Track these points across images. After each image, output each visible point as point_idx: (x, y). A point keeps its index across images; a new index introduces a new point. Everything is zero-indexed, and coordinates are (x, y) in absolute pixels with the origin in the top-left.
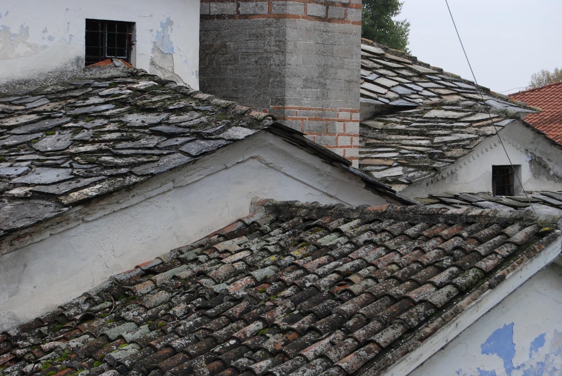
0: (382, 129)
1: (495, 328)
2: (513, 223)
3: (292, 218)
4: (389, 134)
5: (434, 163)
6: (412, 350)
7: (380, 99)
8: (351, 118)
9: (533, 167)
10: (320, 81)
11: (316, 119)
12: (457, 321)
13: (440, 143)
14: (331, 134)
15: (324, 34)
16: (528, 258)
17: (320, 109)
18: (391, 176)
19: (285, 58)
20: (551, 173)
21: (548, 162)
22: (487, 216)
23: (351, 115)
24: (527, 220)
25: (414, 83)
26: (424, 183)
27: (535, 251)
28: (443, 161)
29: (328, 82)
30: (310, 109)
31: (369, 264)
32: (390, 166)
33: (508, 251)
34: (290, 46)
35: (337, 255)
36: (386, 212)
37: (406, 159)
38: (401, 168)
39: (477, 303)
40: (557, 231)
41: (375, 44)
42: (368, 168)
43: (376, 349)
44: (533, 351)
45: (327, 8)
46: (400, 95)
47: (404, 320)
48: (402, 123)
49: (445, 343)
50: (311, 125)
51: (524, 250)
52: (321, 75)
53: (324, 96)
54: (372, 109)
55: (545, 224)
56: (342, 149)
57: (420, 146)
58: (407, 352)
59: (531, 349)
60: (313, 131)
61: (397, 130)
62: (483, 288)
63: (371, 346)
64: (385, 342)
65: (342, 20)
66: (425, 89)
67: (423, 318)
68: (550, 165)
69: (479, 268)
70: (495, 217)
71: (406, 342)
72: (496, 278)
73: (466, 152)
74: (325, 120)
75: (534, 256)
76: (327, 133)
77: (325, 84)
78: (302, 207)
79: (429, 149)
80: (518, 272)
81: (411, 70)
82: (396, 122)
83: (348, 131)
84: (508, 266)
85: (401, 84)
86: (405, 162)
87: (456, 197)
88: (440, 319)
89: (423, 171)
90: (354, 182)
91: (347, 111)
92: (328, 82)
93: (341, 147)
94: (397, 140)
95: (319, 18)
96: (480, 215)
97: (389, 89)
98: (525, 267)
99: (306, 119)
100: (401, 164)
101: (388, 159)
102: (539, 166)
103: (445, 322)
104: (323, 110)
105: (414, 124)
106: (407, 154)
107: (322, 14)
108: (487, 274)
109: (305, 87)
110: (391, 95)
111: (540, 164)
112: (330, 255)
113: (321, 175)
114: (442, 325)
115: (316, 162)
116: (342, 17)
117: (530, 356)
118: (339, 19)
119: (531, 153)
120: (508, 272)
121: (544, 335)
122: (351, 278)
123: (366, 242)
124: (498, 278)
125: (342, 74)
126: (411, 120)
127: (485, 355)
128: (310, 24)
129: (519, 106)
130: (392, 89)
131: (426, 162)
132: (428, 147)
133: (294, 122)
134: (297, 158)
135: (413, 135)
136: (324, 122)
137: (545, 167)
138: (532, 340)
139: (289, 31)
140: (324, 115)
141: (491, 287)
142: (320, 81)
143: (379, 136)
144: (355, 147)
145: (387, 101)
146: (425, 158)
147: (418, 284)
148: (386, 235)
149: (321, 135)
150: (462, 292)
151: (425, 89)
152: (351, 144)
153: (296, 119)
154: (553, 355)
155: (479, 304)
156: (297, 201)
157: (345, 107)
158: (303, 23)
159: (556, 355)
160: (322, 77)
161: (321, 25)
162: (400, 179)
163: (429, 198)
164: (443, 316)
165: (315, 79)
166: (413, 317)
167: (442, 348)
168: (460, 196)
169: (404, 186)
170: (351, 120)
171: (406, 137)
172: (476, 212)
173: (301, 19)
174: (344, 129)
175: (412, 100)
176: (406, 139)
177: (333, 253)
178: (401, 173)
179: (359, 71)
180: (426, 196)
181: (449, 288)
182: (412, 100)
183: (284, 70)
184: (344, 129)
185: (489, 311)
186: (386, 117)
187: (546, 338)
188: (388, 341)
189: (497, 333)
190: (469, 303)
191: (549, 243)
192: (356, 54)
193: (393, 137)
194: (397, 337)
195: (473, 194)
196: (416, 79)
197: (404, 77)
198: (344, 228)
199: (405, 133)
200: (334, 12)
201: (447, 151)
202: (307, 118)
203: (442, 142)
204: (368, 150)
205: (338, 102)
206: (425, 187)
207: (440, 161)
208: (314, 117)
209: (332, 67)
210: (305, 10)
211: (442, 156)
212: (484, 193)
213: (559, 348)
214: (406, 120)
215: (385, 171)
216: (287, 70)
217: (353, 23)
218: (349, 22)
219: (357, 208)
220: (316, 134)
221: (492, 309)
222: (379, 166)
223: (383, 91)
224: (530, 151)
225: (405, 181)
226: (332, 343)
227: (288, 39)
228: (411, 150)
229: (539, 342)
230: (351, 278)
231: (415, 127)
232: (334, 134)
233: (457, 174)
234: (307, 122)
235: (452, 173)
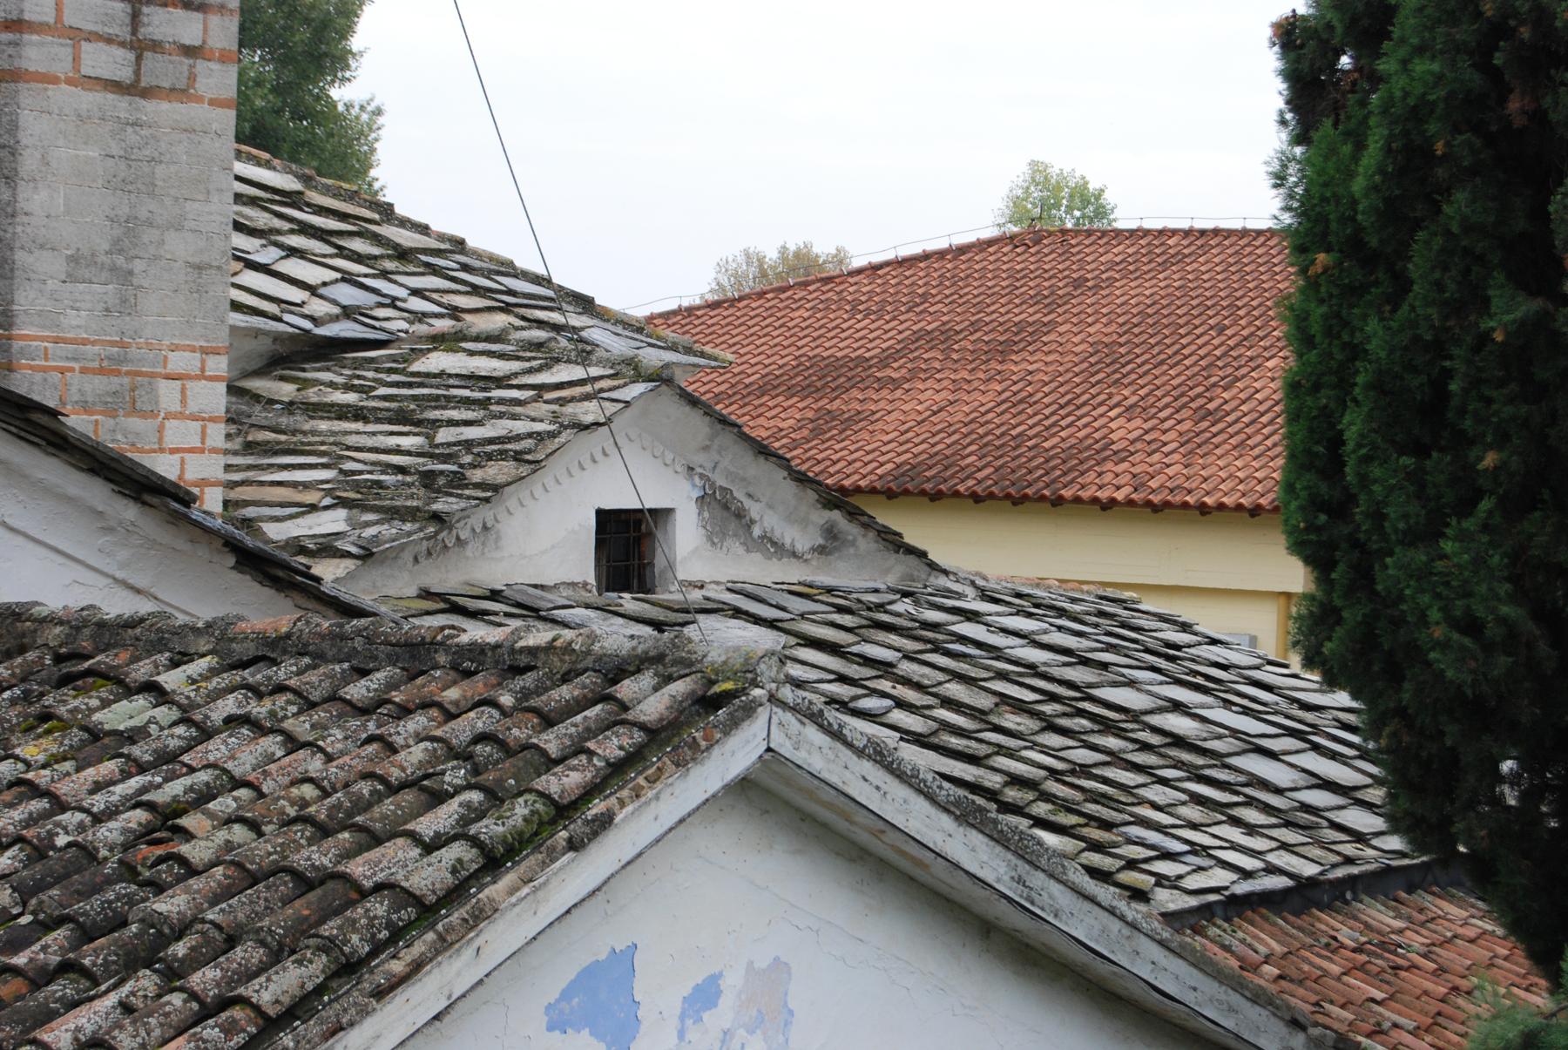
0: (291, 403)
1: (586, 960)
2: (639, 671)
3: (22, 650)
4: (312, 418)
5: (435, 500)
6: (352, 1024)
7: (287, 317)
8: (203, 370)
9: (706, 515)
10: (117, 264)
11: (101, 371)
12: (478, 942)
13: (454, 444)
14: (144, 415)
15: (130, 129)
16: (678, 765)
17: (113, 344)
18: (314, 536)
19: (14, 195)
20: (757, 531)
21: (748, 503)
22: (568, 648)
23: (203, 362)
24: (675, 662)
25: (385, 275)
26: (407, 556)
27: (694, 745)
28: (459, 496)
29: (138, 266)
30: (84, 342)
31: (238, 783)
32: (313, 508)
33: (621, 748)
34: (28, 163)
35: (147, 757)
36: (288, 636)
37: (357, 486)
38: (342, 513)
39: (536, 889)
40: (757, 692)
41: (276, 162)
42: (250, 512)
43: (250, 1021)
44: (689, 1022)
45: (139, 58)
46: (344, 307)
47: (331, 939)
48: (348, 388)
49: (445, 1003)
50: (88, 388)
51: (667, 742)
52: (117, 247)
53: (126, 306)
54: (265, 345)
55: (722, 672)
56: (177, 456)
57: (398, 451)
58: (339, 1029)
59: (682, 1017)
60: (94, 404)
61: (333, 405)
62: (552, 849)
63: (237, 1013)
64: (277, 1001)
65: (181, 93)
66: (416, 292)
67: (384, 934)
68: (754, 509)
69: (541, 794)
70: (588, 652)
71: (336, 1000)
72: (587, 822)
73: (524, 470)
74: (128, 373)
75: (693, 759)
76: (134, 411)
77: (131, 273)
78: (51, 620)
79: (421, 460)
80: (647, 803)
81: (377, 239)
82: (332, 385)
83: (193, 407)
84: (621, 788)
85: (348, 279)
86: (356, 496)
87: (495, 595)
88: (430, 936)
89: (404, 521)
90: (203, 552)
92: (138, 266)
93: (173, 451)
94: (334, 433)
95: (115, 86)
96: (550, 647)
97: (312, 290)
98: (669, 790)
99: (72, 370)
100: (343, 503)
101: (306, 486)
102: (724, 511)
103: (444, 945)
104: (122, 345)
105: (382, 391)
106: (361, 472)
107: (125, 74)
108: (563, 811)
109: (71, 278)
110: (318, 307)
111: (726, 507)
112: (128, 757)
113: (109, 530)
114: (438, 953)
115: (96, 492)
116: (181, 85)
117: (681, 1034)
118: (173, 90)
119: (701, 476)
120: (622, 804)
121: (721, 975)
122: (184, 821)
123: (232, 721)
124: (593, 821)
125: (180, 246)
126: (374, 380)
127: (557, 1032)
129: (673, 348)
130: (322, 291)
131: (412, 496)
132: (419, 455)
133: (38, 376)
134: (41, 481)
135: (379, 421)
136: (126, 380)
137: (740, 514)
138: (687, 990)
139: (27, 118)
140: (125, 360)
141: (574, 845)
142: (117, 264)
143: (284, 421)
144: (214, 451)
145: (307, 325)
146: (410, 485)
147: (376, 840)
148: (289, 702)
149: (114, 417)
150: (494, 861)
151: (416, 292)
153: (44, 369)
154: (742, 1032)
155: (540, 894)
156: (37, 603)
157: (187, 337)
158: (63, 96)
159: (751, 1032)
160: (120, 251)
161: (121, 105)
162: (339, 544)
163: (419, 597)
164: (440, 927)
165: (102, 258)
166: (355, 931)
167: (437, 1017)
168: (507, 593)
169: (350, 564)
170: (202, 376)
171: (359, 426)
172: (539, 636)
173: (63, 86)
174: (183, 401)
175: (377, 324)
176: (358, 433)
177: (136, 751)
178: (341, 527)
179: (227, 237)
180: (412, 591)
181: (457, 851)
182: (377, 324)
183: (10, 230)
184: (183, 401)
185: (568, 912)
186: (304, 370)
187: (724, 984)
188: (286, 1000)
189: (590, 973)
190: (512, 891)
191: (733, 724)
192: (220, 191)
193: (323, 426)
194: (310, 986)
195: (542, 587)
196: (390, 265)
197: (358, 258)
198: (171, 680)
199: (358, 414)
200: (159, 69)
201: (473, 466)
202: (76, 366)
203: (458, 443)
204: (250, 460)
205: (166, 323)
206: (410, 565)
207: (451, 495)
208: (96, 364)
209: (151, 225)
210: (76, 59)
211: (458, 481)
212: (573, 585)
213: (759, 1011)
214: (359, 377)
215: (299, 521)
216: (19, 229)
217: (212, 102)
218: (199, 99)
219: (209, 625)
221: (575, 906)
222: (282, 505)
223: (296, 295)
224: (699, 470)
225: (354, 550)
226: (126, 1008)
227: (24, 141)
228: (373, 464)
229: (705, 996)
230: (184, 821)
231: (385, 398)
232: (153, 414)
233: (498, 532)
234: (75, 379)
235: (485, 528)
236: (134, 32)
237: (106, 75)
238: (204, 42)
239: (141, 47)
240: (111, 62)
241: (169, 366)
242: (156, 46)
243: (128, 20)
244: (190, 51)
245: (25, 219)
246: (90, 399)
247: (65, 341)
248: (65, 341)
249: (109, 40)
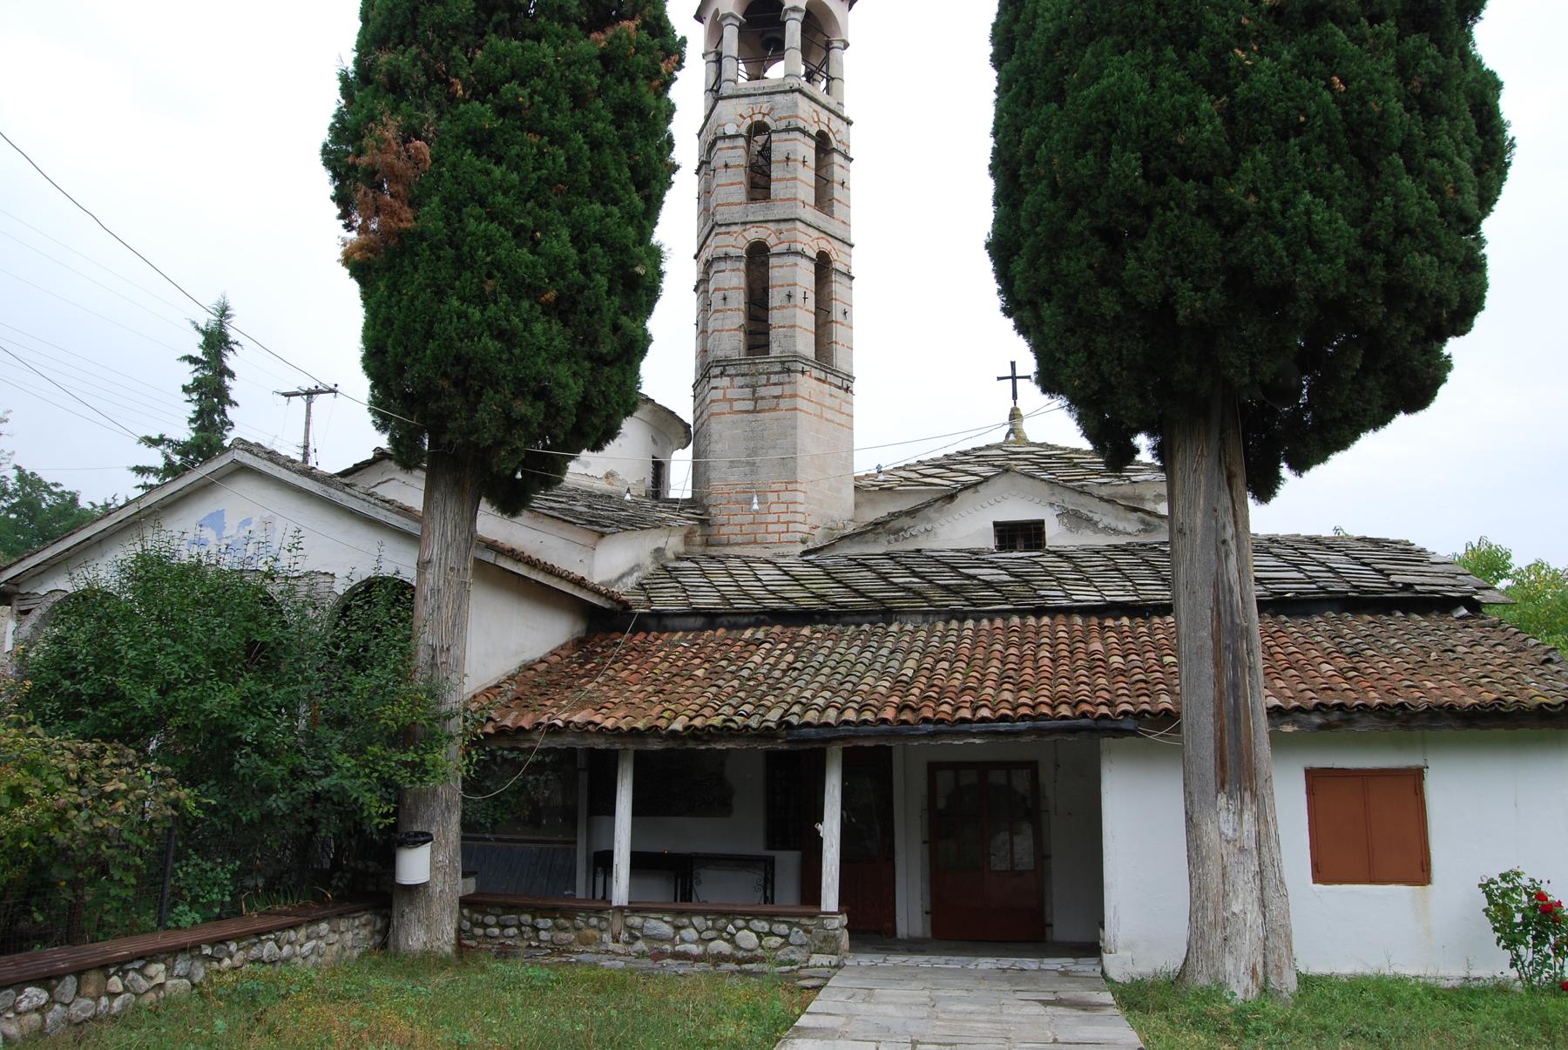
34: (715, 437)
65: (774, 410)
68: (1096, 518)
95: (747, 412)
137: (1089, 520)
161: (750, 417)
239: (756, 400)
240: (749, 405)
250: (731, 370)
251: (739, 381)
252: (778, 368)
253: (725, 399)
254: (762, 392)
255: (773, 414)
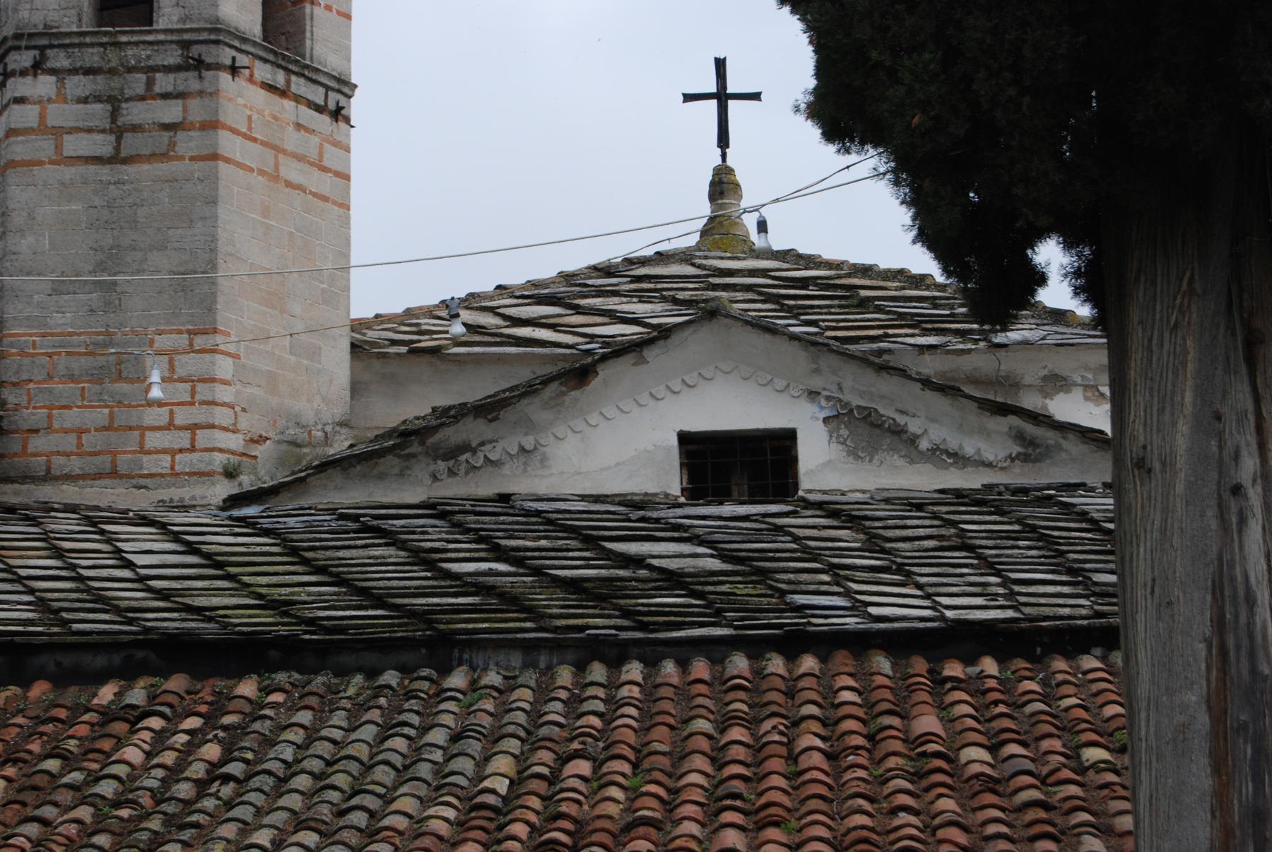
9: (844, 432)
14: (129, 380)
15: (112, 187)
20: (924, 445)
21: (901, 420)
30: (71, 334)
34: (18, 219)
45: (119, 139)
52: (100, 267)
60: (81, 375)
65: (164, 156)
68: (914, 426)
76: (120, 377)
83: (180, 372)
91: (180, 332)
102: (864, 429)
104: (107, 333)
107: (107, 150)
111: (873, 425)
116: (163, 149)
118: (153, 155)
119: (828, 398)
128: (69, 172)
133: (26, 361)
137: (898, 432)
152: (193, 396)
153: (33, 355)
157: (173, 324)
161: (105, 172)
200: (131, 143)
205: (153, 316)
209: (134, 249)
217: (192, 159)
218: (182, 158)
220: (88, 382)
224: (825, 393)
227: (12, 206)
235: (523, 450)
236: (114, 121)
237: (87, 154)
238: (184, 119)
239: (118, 131)
240: (102, 144)
241: (156, 345)
242: (135, 128)
243: (108, 114)
244: (167, 127)
245: (13, 257)
246: (76, 373)
247: (52, 335)
248: (52, 335)
249: (89, 130)
250: (59, 60)
251: (78, 85)
252: (173, 57)
253: (43, 129)
254: (135, 113)
255: (161, 168)
